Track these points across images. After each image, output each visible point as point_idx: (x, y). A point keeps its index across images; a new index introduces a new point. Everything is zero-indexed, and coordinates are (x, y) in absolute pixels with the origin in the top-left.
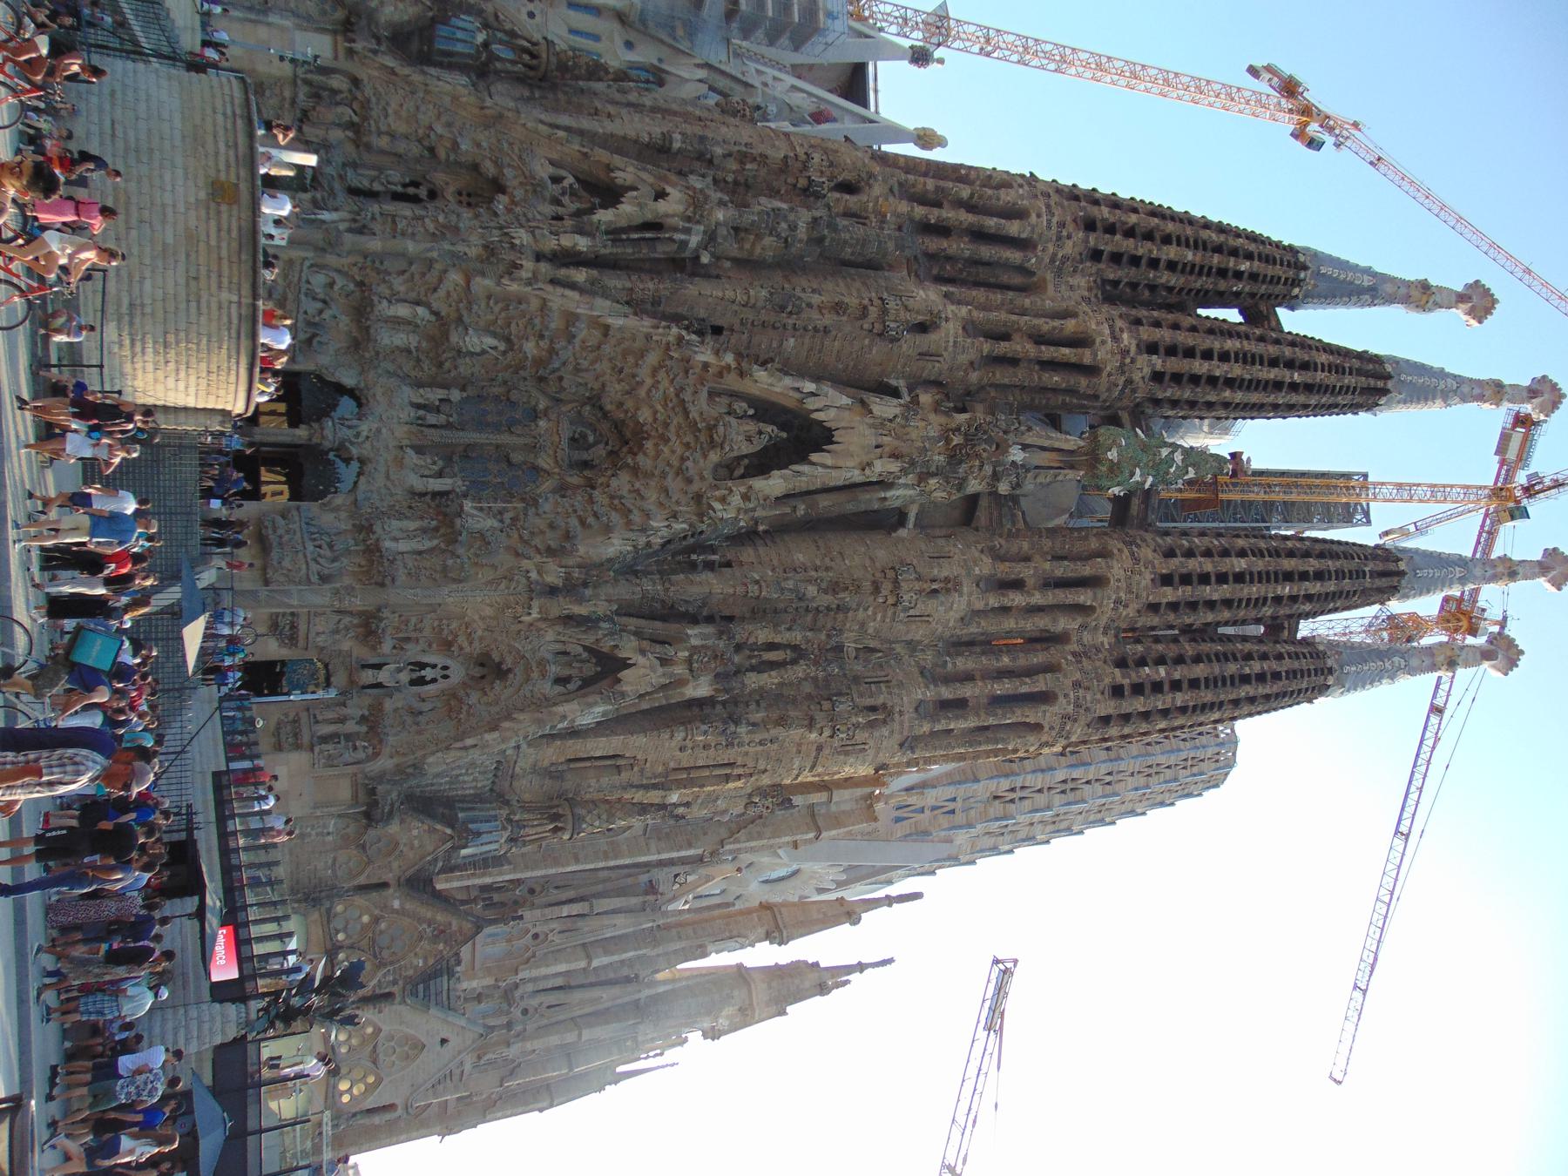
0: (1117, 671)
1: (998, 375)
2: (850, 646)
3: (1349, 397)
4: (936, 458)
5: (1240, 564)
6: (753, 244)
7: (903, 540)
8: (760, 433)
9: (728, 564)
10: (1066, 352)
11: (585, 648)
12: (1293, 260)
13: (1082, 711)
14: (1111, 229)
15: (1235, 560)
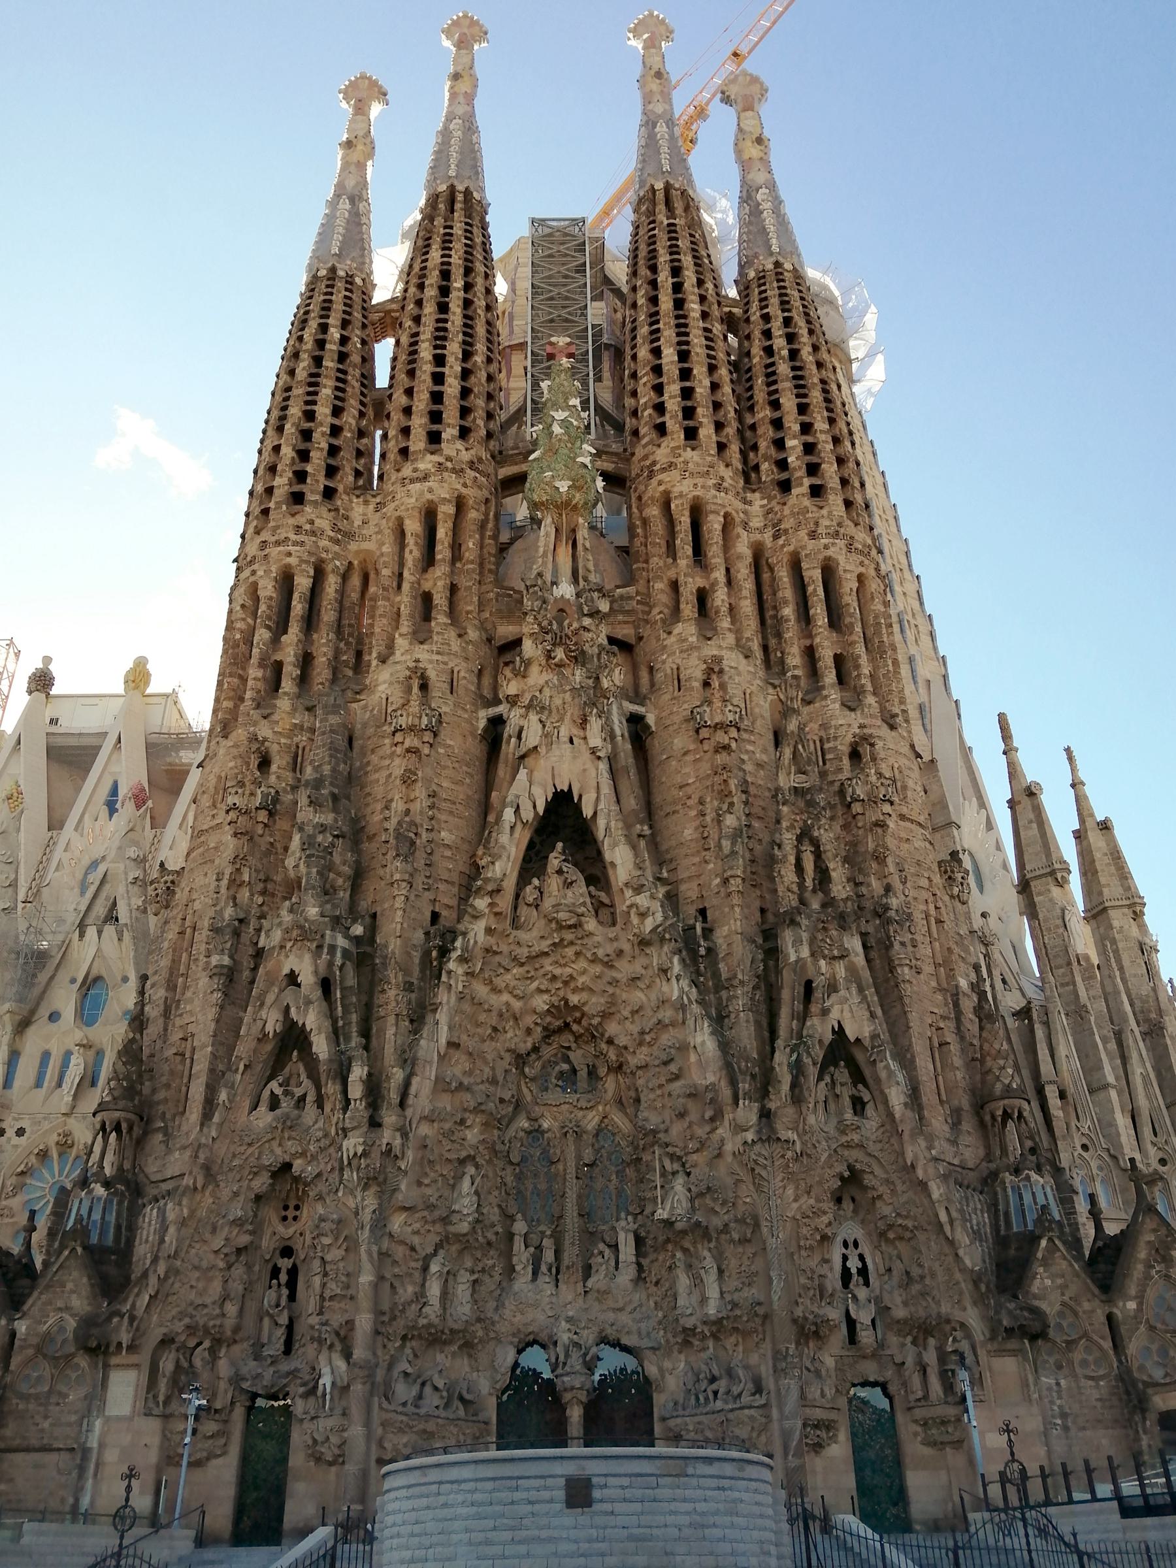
0: (795, 491)
1: (469, 608)
2: (796, 780)
3: (475, 230)
4: (578, 678)
5: (669, 355)
6: (339, 874)
7: (659, 719)
8: (560, 872)
9: (703, 912)
10: (443, 532)
11: (820, 1078)
12: (325, 282)
13: (842, 531)
14: (301, 476)
15: (664, 361)
